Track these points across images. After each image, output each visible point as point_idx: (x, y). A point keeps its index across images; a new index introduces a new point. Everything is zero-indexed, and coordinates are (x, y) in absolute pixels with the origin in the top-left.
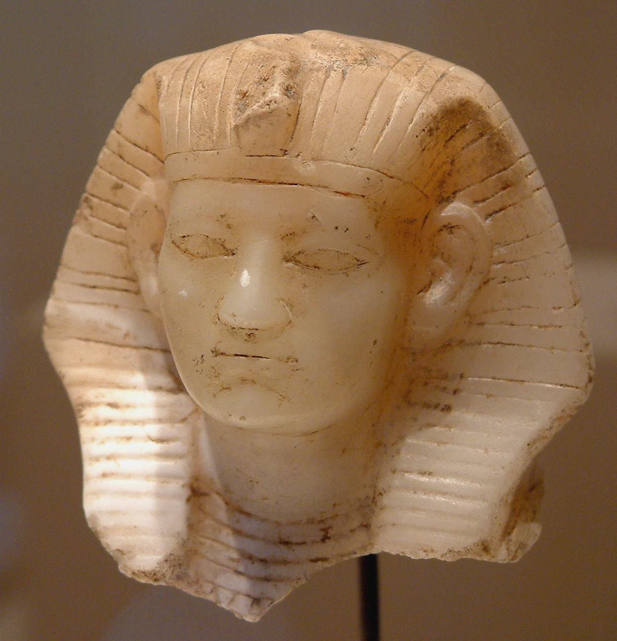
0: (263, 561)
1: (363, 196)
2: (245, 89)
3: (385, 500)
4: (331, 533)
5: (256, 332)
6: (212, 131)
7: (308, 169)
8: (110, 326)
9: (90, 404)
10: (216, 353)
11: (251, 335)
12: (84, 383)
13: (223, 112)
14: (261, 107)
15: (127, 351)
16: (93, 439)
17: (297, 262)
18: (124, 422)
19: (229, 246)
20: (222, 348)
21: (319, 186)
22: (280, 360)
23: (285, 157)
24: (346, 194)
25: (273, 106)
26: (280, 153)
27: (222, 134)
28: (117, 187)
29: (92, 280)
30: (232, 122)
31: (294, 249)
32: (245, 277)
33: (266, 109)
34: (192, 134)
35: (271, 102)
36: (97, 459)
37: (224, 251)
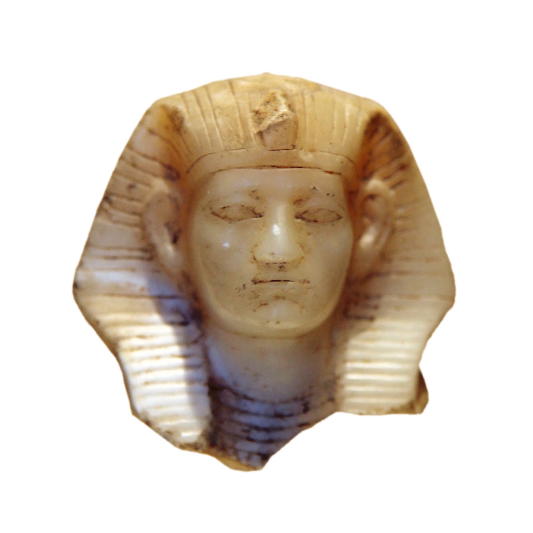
0: (267, 430)
1: (339, 174)
2: (257, 108)
3: (342, 382)
4: (310, 406)
5: (284, 265)
6: (238, 136)
7: (307, 157)
8: (129, 285)
9: (124, 338)
10: (255, 282)
11: (282, 267)
12: (116, 324)
13: (244, 124)
14: (277, 118)
15: (143, 301)
16: (132, 361)
17: (303, 219)
18: (152, 347)
19: (258, 211)
20: (260, 277)
21: (315, 168)
22: (300, 281)
23: (295, 150)
24: (331, 173)
25: (285, 117)
26: (292, 147)
27: (248, 139)
28: (131, 187)
29: (113, 253)
30: (253, 130)
31: (301, 209)
32: (277, 230)
33: (280, 120)
34: (223, 140)
35: (283, 114)
36: (138, 373)
37: (253, 215)
